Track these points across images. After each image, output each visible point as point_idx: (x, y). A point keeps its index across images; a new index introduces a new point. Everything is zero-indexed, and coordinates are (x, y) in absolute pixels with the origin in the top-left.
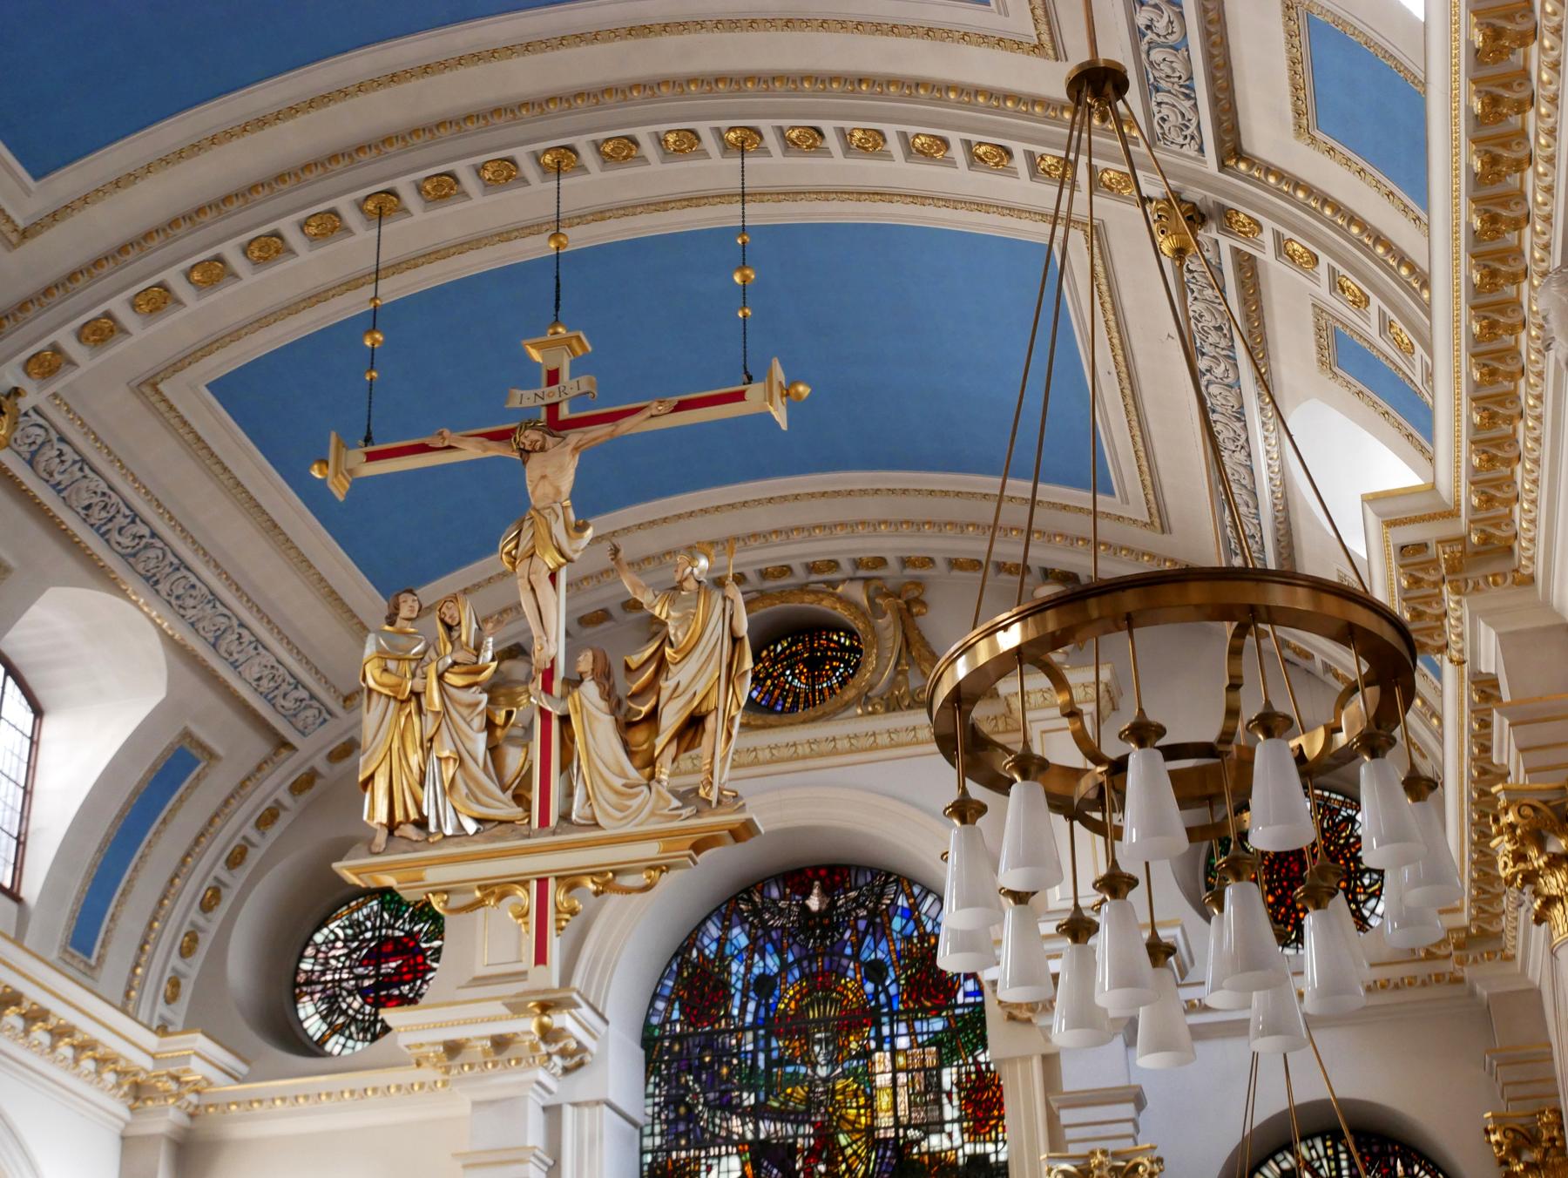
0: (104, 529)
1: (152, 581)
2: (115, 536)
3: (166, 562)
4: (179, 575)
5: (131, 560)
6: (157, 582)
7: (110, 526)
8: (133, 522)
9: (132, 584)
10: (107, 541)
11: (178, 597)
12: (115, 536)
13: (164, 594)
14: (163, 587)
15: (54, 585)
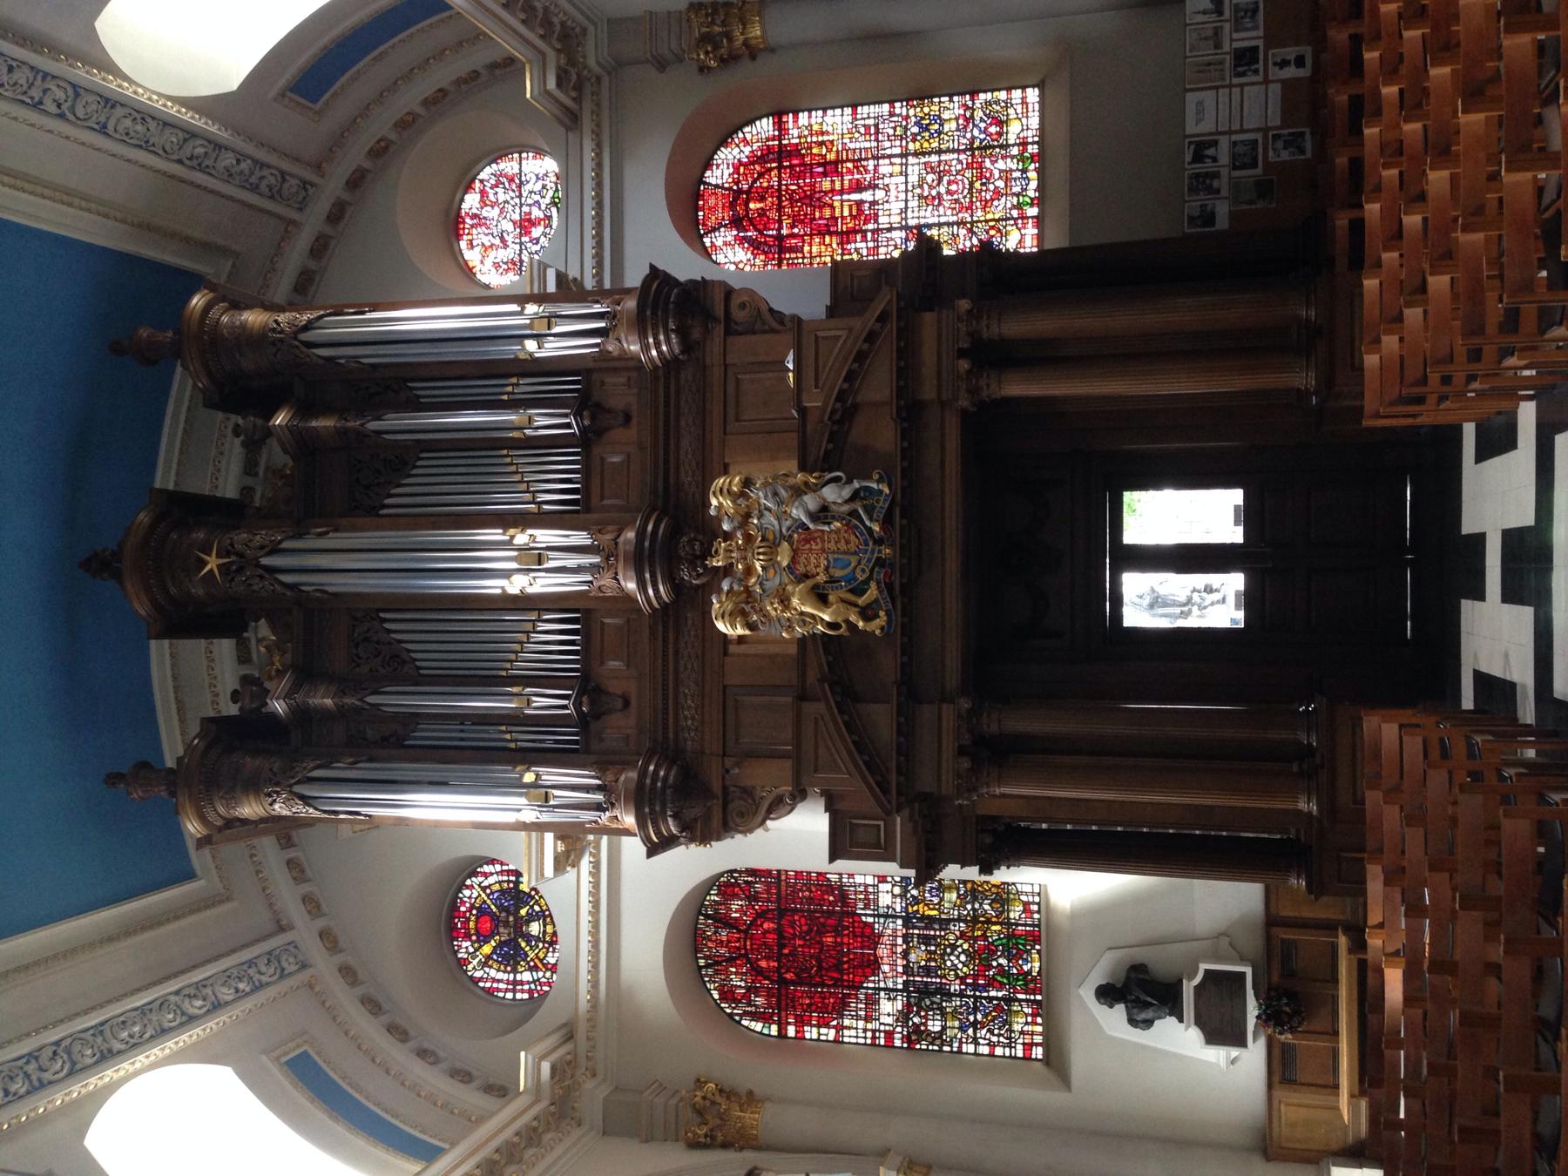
0: (36, 1083)
1: (107, 1056)
2: (47, 1076)
3: (91, 1039)
4: (108, 1033)
5: (78, 1066)
6: (110, 1051)
7: (34, 1077)
8: (37, 1058)
9: (109, 1074)
10: (50, 1083)
11: (131, 1036)
12: (47, 1076)
13: (123, 1047)
14: (117, 1046)
15: (83, 1137)
